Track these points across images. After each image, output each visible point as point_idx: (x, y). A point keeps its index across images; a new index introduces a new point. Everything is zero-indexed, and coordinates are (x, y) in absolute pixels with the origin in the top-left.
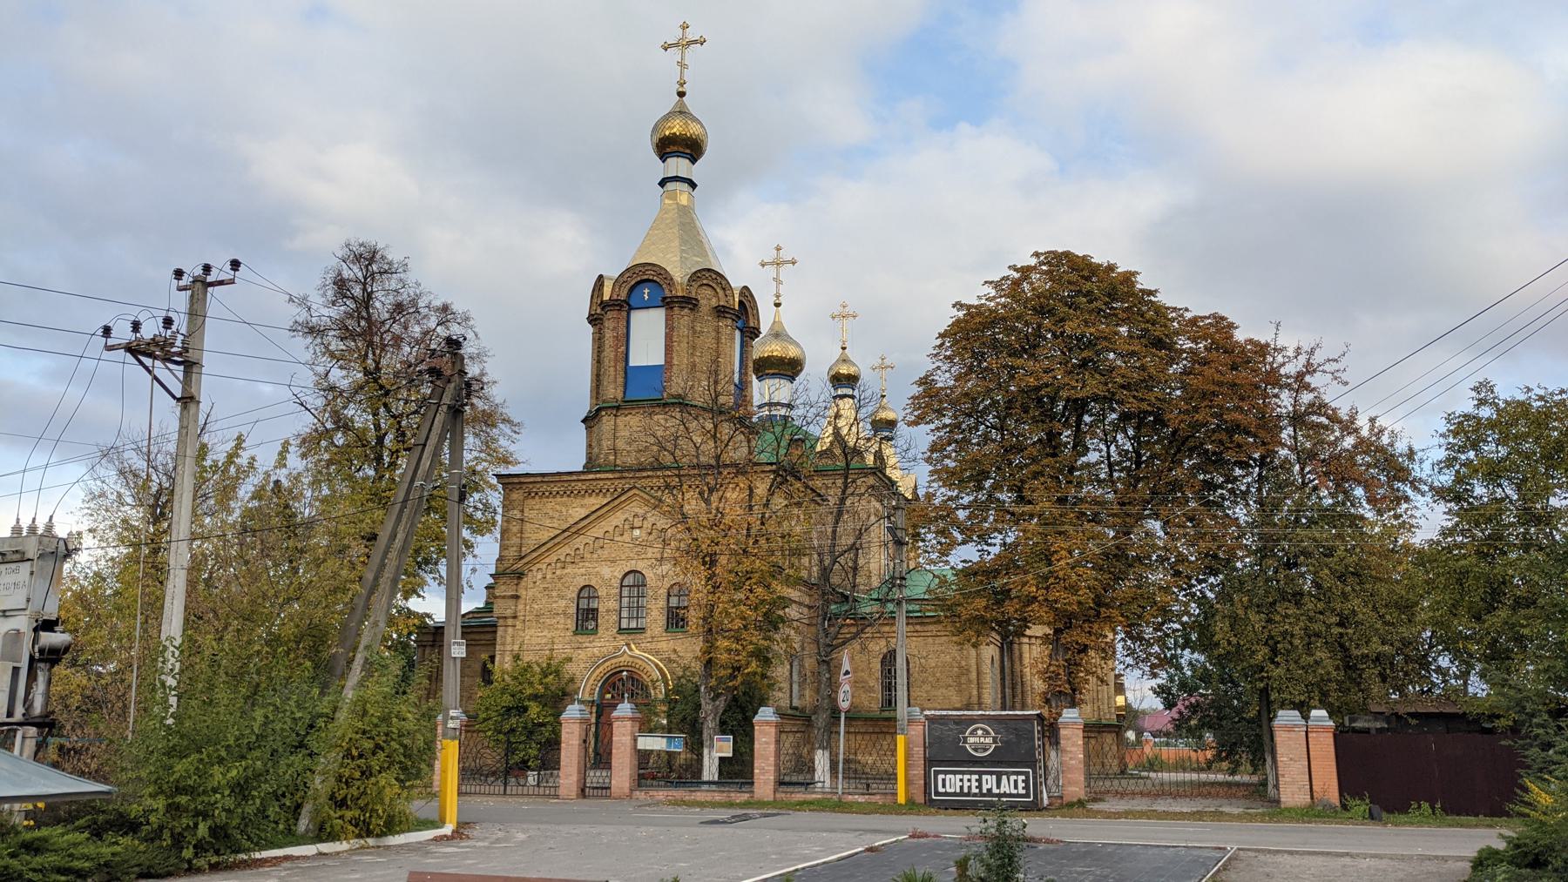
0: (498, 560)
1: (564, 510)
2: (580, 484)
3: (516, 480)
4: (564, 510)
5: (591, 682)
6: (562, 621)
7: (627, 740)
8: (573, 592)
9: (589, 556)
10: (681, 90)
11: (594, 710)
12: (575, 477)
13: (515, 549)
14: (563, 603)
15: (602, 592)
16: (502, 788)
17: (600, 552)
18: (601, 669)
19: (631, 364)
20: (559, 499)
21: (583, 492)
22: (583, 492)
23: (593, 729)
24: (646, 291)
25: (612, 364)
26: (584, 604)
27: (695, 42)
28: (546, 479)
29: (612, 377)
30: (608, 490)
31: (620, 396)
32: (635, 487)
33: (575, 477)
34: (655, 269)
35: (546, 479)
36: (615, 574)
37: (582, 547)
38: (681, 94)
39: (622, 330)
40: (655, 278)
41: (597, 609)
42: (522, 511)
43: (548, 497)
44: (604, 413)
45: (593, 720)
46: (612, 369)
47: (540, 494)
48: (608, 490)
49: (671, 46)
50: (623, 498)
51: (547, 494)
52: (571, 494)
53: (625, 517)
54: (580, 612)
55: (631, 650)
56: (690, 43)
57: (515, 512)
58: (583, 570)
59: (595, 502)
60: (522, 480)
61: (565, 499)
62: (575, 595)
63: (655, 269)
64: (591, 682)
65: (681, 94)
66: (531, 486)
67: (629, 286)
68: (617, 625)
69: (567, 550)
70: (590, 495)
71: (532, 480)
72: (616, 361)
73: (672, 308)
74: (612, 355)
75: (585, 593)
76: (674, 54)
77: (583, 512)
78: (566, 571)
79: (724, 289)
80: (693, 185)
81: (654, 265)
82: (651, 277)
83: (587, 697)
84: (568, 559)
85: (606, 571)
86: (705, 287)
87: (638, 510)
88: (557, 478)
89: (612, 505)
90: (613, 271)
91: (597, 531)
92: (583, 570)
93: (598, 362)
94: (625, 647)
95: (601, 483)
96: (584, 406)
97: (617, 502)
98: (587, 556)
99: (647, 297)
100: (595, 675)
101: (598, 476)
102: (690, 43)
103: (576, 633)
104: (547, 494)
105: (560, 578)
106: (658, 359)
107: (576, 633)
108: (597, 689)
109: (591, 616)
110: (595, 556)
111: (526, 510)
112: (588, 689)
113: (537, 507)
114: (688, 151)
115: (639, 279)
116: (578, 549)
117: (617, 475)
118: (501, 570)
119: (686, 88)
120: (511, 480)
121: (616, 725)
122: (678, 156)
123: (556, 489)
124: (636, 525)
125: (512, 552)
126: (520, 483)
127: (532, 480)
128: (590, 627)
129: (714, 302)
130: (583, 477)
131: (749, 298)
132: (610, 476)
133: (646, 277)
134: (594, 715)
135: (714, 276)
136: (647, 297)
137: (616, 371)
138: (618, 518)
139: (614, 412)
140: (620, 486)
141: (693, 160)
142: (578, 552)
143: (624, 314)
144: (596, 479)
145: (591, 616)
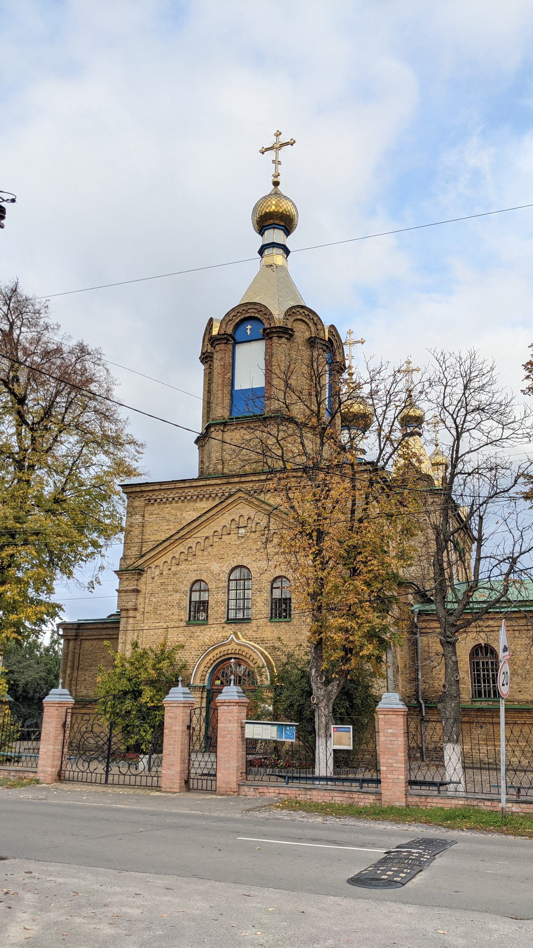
0: (121, 559)
1: (179, 513)
2: (192, 490)
3: (138, 489)
4: (179, 513)
5: (202, 668)
6: (176, 613)
7: (234, 727)
8: (186, 586)
9: (200, 553)
10: (276, 180)
11: (205, 695)
12: (188, 484)
13: (136, 548)
14: (177, 596)
15: (212, 586)
16: (104, 777)
17: (210, 549)
18: (211, 656)
19: (237, 387)
20: (174, 505)
21: (195, 498)
22: (195, 498)
23: (204, 714)
24: (249, 327)
25: (220, 388)
26: (195, 597)
27: (287, 144)
28: (163, 487)
29: (220, 399)
30: (217, 495)
31: (226, 414)
32: (239, 490)
33: (188, 484)
34: (256, 307)
35: (163, 487)
36: (224, 569)
37: (194, 546)
38: (276, 184)
39: (229, 360)
40: (256, 315)
41: (207, 602)
42: (143, 516)
43: (165, 503)
44: (212, 429)
45: (204, 705)
46: (220, 392)
47: (158, 501)
48: (217, 495)
49: (267, 149)
50: (230, 501)
51: (164, 500)
52: (184, 499)
53: (231, 518)
54: (193, 604)
55: (238, 638)
56: (283, 145)
57: (137, 517)
58: (195, 567)
59: (206, 505)
60: (143, 489)
61: (180, 504)
62: (188, 589)
63: (256, 307)
64: (202, 668)
65: (276, 184)
66: (150, 494)
67: (234, 323)
68: (226, 616)
69: (181, 548)
70: (201, 500)
71: (151, 488)
72: (223, 385)
73: (271, 338)
74: (220, 381)
75: (196, 587)
76: (271, 155)
77: (195, 515)
78: (180, 567)
79: (315, 324)
80: (287, 252)
81: (255, 304)
82: (253, 315)
83: (198, 683)
84: (183, 557)
85: (215, 567)
86: (299, 322)
87: (242, 512)
88: (172, 486)
89: (220, 507)
90: (219, 315)
91: (207, 531)
92: (195, 567)
93: (209, 392)
94: (233, 636)
95: (211, 489)
96: (199, 428)
97: (224, 504)
98: (199, 553)
99: (249, 332)
100: (206, 661)
101: (208, 482)
102: (283, 145)
103: (189, 624)
104: (164, 500)
105: (174, 575)
106: (259, 382)
107: (189, 624)
108: (208, 675)
109: (202, 608)
110: (206, 553)
111: (147, 515)
112: (199, 676)
113: (156, 512)
114: (283, 224)
115: (242, 317)
116: (191, 547)
117: (224, 481)
118: (124, 567)
119: (279, 179)
120: (134, 489)
121: (221, 710)
122: (274, 228)
123: (172, 496)
124: (241, 525)
125: (134, 551)
126: (142, 491)
127: (151, 488)
128: (201, 618)
129: (307, 335)
130: (195, 484)
131: (336, 338)
132: (218, 482)
133: (248, 315)
134: (205, 700)
135: (307, 313)
136: (249, 332)
137: (223, 394)
138: (225, 519)
139: (222, 428)
140: (227, 490)
141: (288, 232)
142: (190, 550)
143: (230, 347)
144: (206, 485)
145: (202, 608)
